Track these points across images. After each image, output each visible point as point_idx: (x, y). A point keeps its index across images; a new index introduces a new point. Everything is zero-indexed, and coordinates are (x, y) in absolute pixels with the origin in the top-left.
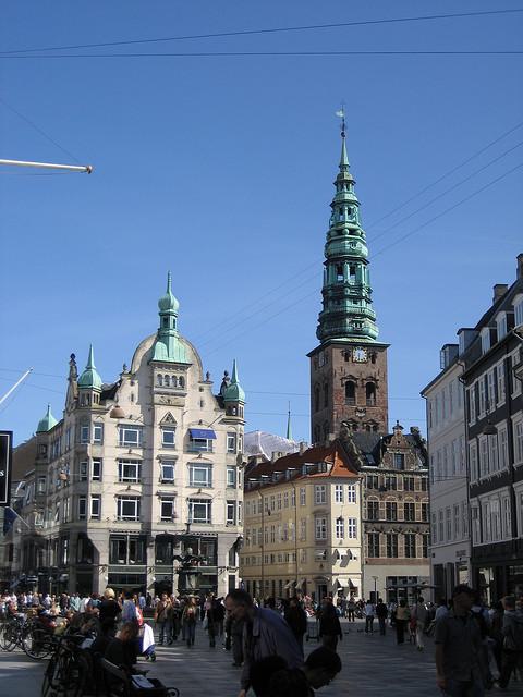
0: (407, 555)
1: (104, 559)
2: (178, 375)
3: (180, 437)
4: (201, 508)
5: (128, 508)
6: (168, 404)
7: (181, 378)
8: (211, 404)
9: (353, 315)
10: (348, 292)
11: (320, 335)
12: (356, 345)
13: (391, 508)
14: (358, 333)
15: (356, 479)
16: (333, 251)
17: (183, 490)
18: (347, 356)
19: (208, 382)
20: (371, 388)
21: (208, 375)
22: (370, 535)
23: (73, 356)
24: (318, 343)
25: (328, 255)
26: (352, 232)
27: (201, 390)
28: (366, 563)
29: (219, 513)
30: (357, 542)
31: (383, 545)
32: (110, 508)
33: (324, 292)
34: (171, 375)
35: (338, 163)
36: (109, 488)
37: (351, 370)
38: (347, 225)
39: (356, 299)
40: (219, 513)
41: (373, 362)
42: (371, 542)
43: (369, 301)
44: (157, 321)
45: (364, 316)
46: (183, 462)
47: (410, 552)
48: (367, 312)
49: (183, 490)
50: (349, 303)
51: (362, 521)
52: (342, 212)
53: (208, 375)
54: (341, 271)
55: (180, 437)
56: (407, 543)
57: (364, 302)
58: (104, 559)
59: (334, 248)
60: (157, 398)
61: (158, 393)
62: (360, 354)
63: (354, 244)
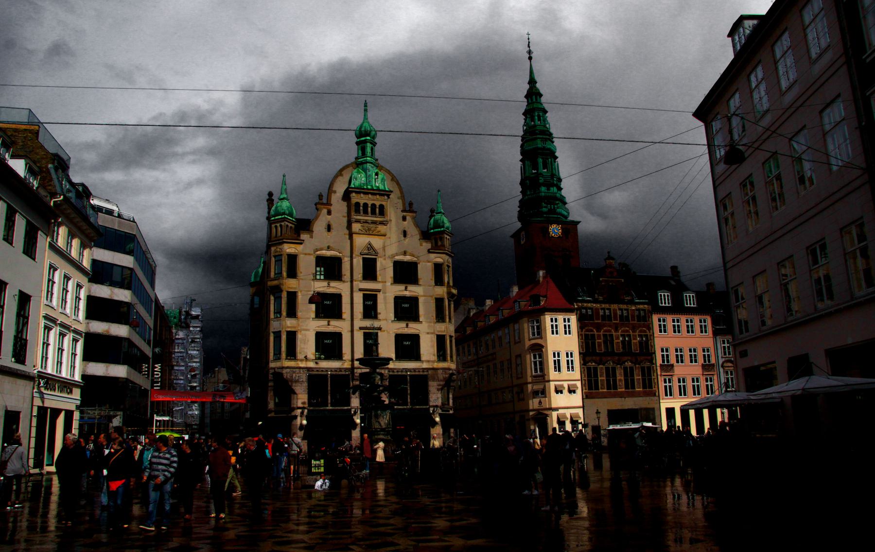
0: (627, 387)
1: (301, 398)
2: (378, 204)
3: (385, 269)
4: (408, 347)
5: (329, 345)
6: (368, 232)
7: (382, 207)
9: (546, 197)
10: (542, 180)
13: (609, 340)
14: (553, 211)
15: (570, 311)
17: (389, 328)
19: (411, 211)
21: (411, 204)
22: (589, 369)
27: (404, 219)
28: (586, 397)
29: (428, 348)
30: (577, 374)
31: (602, 378)
32: (307, 346)
33: (522, 183)
34: (370, 203)
35: (528, 79)
36: (308, 327)
38: (538, 128)
39: (549, 185)
40: (428, 348)
42: (589, 375)
44: (353, 152)
45: (556, 198)
46: (388, 292)
47: (630, 384)
48: (558, 195)
49: (389, 328)
51: (580, 353)
54: (535, 167)
55: (385, 269)
56: (626, 375)
57: (555, 189)
58: (301, 398)
60: (356, 227)
61: (358, 221)
62: (555, 230)
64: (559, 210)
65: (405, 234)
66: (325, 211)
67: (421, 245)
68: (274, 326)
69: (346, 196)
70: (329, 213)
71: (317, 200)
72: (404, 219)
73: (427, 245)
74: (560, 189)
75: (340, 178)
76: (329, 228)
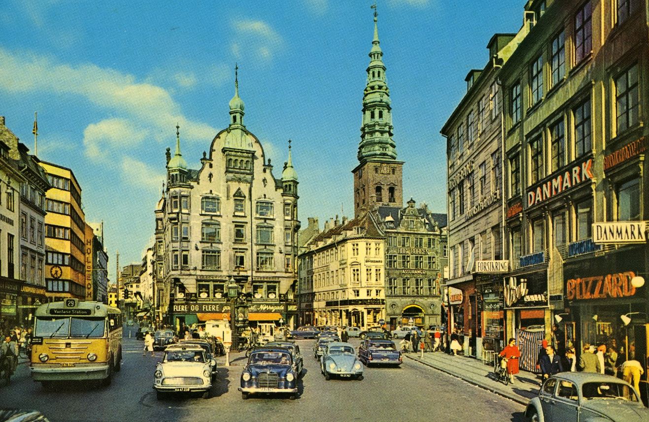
8: (271, 184)
11: (360, 159)
12: (382, 162)
16: (368, 101)
18: (376, 170)
20: (392, 190)
21: (269, 160)
24: (358, 163)
25: (365, 105)
26: (380, 87)
27: (265, 171)
37: (379, 177)
39: (382, 133)
41: (393, 173)
43: (391, 135)
48: (389, 140)
50: (378, 134)
52: (374, 76)
53: (269, 160)
54: (373, 116)
59: (370, 98)
62: (385, 169)
63: (382, 96)
64: (390, 153)
65: (264, 180)
70: (211, 166)
71: (202, 157)
72: (265, 171)
73: (281, 191)
74: (391, 135)
76: (211, 176)
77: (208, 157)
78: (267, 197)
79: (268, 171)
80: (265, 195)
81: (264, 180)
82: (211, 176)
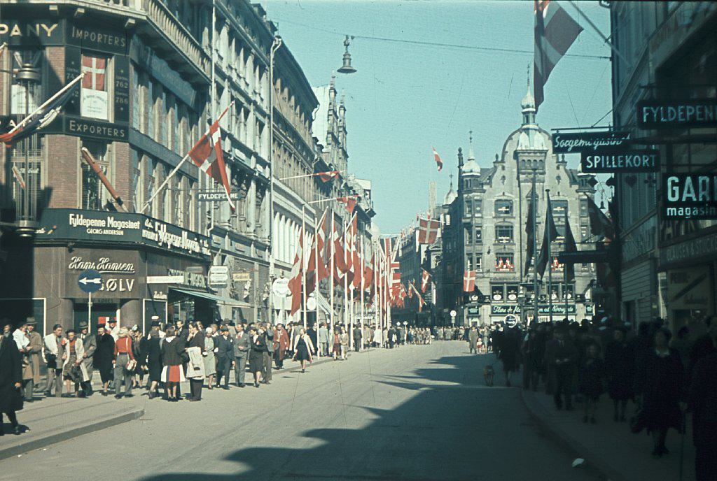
8: (566, 180)
23: (460, 150)
27: (558, 168)
32: (489, 260)
61: (524, 174)
66: (500, 168)
67: (571, 187)
68: (467, 249)
69: (516, 154)
70: (503, 168)
71: (495, 160)
72: (558, 168)
75: (510, 142)
76: (504, 178)
77: (500, 159)
78: (561, 194)
79: (561, 167)
80: (559, 193)
81: (559, 178)
82: (504, 178)
